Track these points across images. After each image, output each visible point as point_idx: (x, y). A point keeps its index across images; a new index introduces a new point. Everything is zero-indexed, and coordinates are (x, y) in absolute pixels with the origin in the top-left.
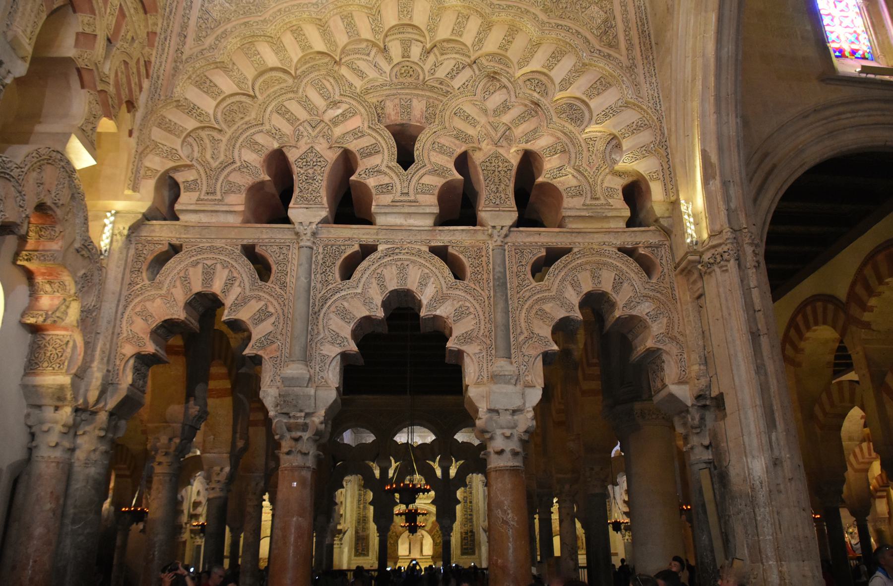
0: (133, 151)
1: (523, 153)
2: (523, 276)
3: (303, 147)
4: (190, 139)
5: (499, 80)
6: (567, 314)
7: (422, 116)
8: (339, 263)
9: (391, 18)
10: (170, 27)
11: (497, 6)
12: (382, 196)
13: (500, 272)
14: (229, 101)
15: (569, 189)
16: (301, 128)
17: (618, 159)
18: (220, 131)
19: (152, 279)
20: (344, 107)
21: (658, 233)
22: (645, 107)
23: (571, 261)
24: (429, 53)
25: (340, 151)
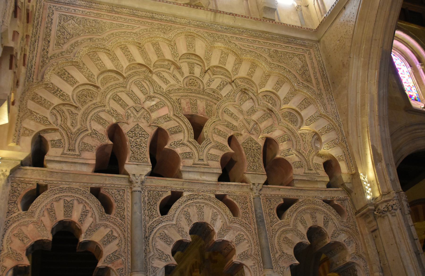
0: (16, 116)
1: (265, 139)
2: (272, 216)
3: (132, 125)
4: (54, 111)
5: (248, 94)
6: (301, 241)
7: (204, 111)
8: (159, 203)
9: (182, 49)
10: (38, 34)
11: (244, 50)
12: (186, 160)
14: (81, 88)
15: (295, 163)
16: (129, 111)
17: (319, 147)
18: (76, 107)
21: (343, 192)
22: (331, 118)
23: (299, 207)
24: (205, 73)
25: (155, 129)
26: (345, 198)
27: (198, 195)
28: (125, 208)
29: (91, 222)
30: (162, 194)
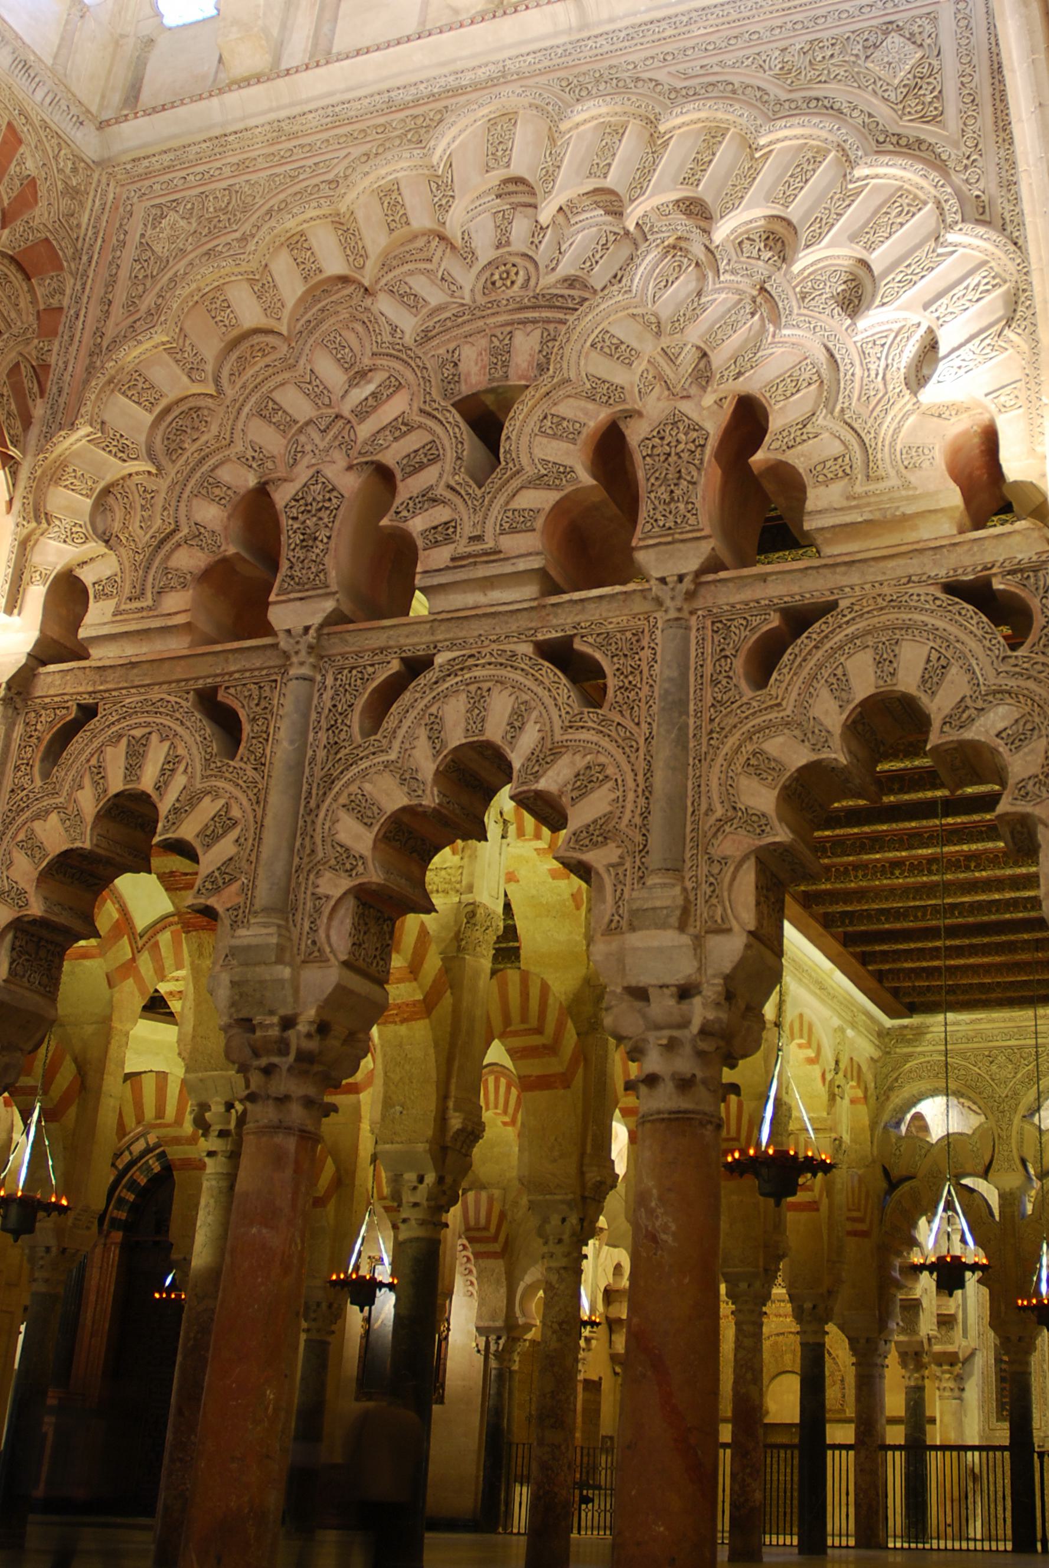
6: (814, 757)
8: (360, 703)
13: (670, 680)
16: (302, 439)
19: (46, 775)
20: (379, 377)
23: (832, 632)
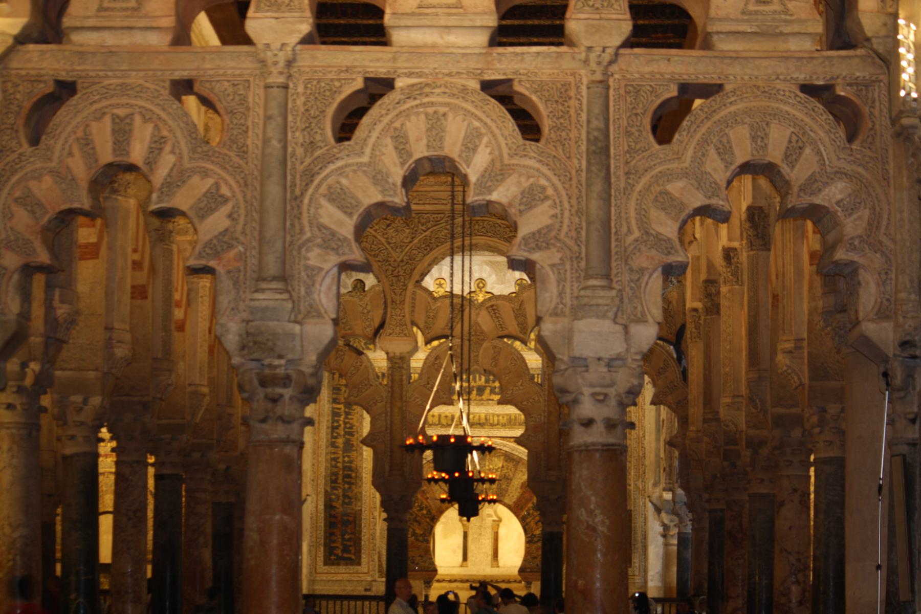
2: (637, 134)
6: (707, 202)
8: (331, 111)
13: (598, 129)
21: (869, 60)
23: (719, 109)
26: (874, 78)
27: (433, 85)
28: (247, 128)
29: (171, 165)
30: (341, 86)
